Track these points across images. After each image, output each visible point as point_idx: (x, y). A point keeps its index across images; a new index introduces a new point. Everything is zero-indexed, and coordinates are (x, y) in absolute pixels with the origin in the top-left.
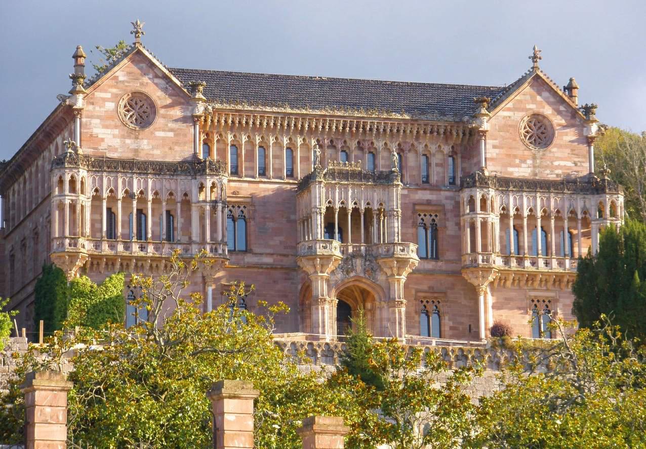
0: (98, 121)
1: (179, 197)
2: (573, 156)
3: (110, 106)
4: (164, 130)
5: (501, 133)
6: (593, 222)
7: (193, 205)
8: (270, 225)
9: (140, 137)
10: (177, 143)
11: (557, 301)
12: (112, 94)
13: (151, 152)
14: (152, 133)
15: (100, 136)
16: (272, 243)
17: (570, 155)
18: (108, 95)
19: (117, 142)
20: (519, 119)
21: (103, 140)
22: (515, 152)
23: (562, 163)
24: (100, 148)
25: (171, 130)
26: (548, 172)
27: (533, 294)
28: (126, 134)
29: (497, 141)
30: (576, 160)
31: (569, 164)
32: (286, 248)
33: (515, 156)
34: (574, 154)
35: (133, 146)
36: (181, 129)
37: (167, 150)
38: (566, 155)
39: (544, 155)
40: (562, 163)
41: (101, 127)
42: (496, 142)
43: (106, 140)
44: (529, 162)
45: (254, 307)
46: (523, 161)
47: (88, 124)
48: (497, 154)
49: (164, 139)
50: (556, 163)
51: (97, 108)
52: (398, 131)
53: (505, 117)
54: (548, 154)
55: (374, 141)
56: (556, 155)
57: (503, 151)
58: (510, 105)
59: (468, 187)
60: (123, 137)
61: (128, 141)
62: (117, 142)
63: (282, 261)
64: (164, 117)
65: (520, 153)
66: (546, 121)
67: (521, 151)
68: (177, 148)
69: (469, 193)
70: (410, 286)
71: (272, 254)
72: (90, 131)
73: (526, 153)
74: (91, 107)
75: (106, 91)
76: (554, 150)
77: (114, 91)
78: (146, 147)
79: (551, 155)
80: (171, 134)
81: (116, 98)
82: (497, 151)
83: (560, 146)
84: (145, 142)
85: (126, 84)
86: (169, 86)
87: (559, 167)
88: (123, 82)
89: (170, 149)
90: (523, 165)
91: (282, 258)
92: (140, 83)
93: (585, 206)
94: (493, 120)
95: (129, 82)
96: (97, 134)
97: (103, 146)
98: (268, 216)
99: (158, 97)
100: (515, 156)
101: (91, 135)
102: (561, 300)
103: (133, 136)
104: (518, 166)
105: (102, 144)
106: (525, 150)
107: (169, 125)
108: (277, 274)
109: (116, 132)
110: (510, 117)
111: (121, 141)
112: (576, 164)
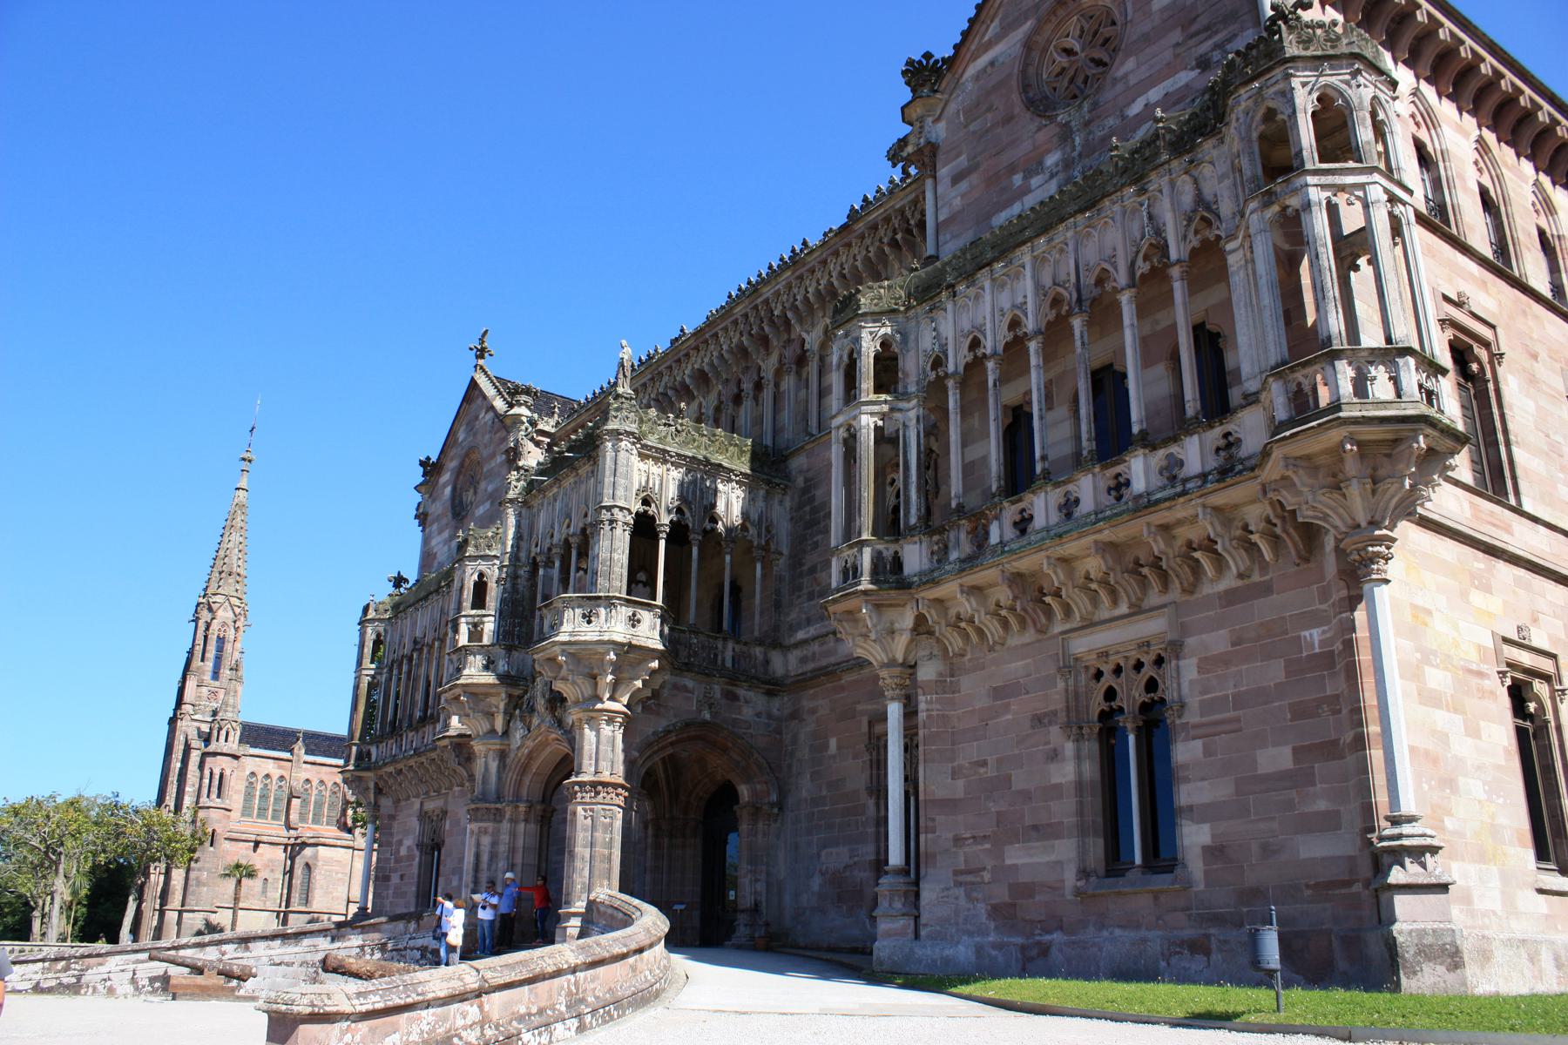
2: (1192, 42)
3: (448, 490)
5: (972, 127)
6: (1229, 247)
11: (1176, 648)
17: (1179, 51)
20: (1018, 49)
22: (1006, 159)
23: (1154, 94)
27: (1082, 645)
29: (963, 157)
30: (1205, 47)
31: (1185, 77)
33: (1012, 169)
34: (1198, 33)
38: (1168, 55)
39: (1095, 106)
40: (1154, 94)
42: (963, 161)
46: (1033, 166)
48: (963, 196)
50: (1136, 108)
53: (977, 78)
54: (1108, 95)
55: (804, 335)
56: (1133, 80)
57: (974, 178)
58: (994, 27)
65: (1026, 146)
67: (1031, 133)
70: (859, 707)
76: (1131, 64)
79: (1120, 87)
80: (487, 505)
82: (963, 186)
83: (1147, 39)
90: (1035, 181)
93: (1199, 199)
94: (952, 107)
102: (1191, 642)
104: (1025, 191)
106: (1039, 129)
110: (992, 64)
112: (1204, 64)
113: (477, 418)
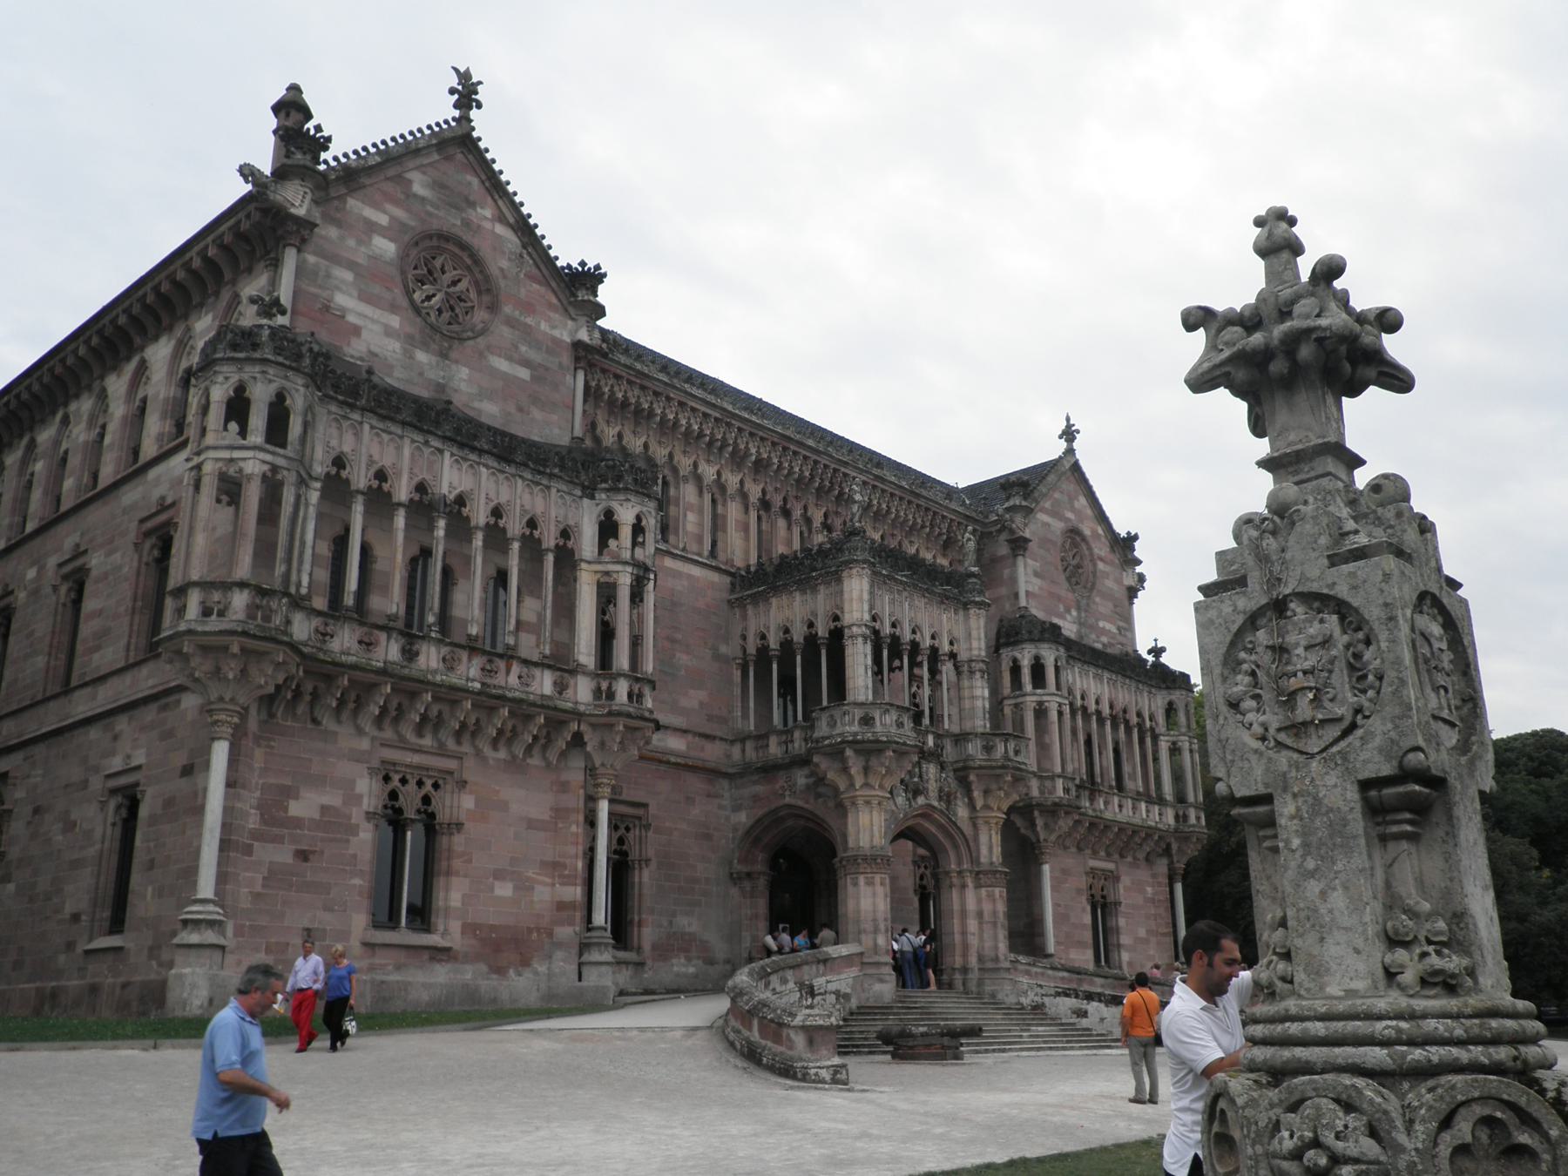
0: (348, 276)
1: (550, 539)
4: (510, 359)
7: (584, 565)
8: (683, 659)
9: (454, 355)
10: (535, 400)
12: (392, 218)
13: (476, 404)
14: (481, 355)
15: (351, 318)
16: (684, 702)
18: (383, 220)
19: (391, 348)
21: (356, 331)
23: (1108, 626)
24: (347, 350)
25: (526, 363)
26: (1093, 636)
28: (417, 336)
32: (710, 718)
35: (434, 375)
36: (547, 369)
37: (513, 410)
41: (355, 293)
43: (364, 334)
44: (1074, 613)
45: (648, 861)
47: (322, 273)
49: (505, 377)
50: (1101, 624)
51: (351, 243)
52: (888, 511)
53: (1047, 525)
56: (1102, 609)
58: (1047, 505)
59: (1032, 640)
60: (409, 340)
61: (421, 356)
62: (391, 348)
63: (702, 749)
64: (511, 323)
66: (1084, 547)
68: (537, 414)
69: (1034, 651)
71: (685, 732)
72: (325, 294)
73: (1070, 595)
74: (333, 232)
75: (376, 206)
77: (399, 213)
78: (463, 386)
80: (524, 374)
81: (394, 231)
82: (1037, 581)
84: (464, 372)
85: (429, 208)
86: (529, 254)
87: (1104, 632)
88: (423, 199)
89: (520, 410)
91: (703, 742)
92: (462, 219)
95: (437, 208)
96: (344, 310)
97: (355, 350)
98: (679, 636)
99: (502, 270)
100: (1059, 599)
101: (326, 308)
103: (435, 347)
105: (354, 341)
107: (523, 349)
108: (695, 783)
109: (395, 321)
111: (405, 351)
112: (1119, 629)
113: (472, 205)
